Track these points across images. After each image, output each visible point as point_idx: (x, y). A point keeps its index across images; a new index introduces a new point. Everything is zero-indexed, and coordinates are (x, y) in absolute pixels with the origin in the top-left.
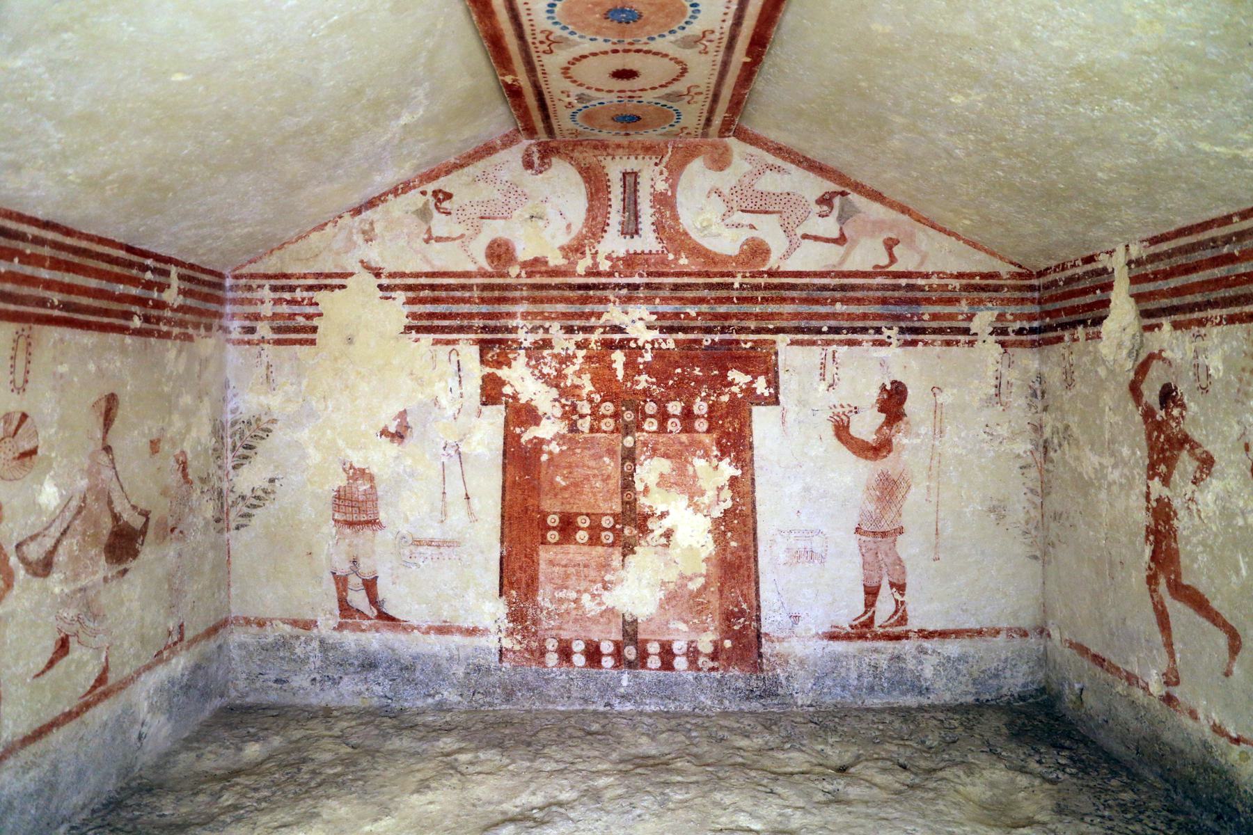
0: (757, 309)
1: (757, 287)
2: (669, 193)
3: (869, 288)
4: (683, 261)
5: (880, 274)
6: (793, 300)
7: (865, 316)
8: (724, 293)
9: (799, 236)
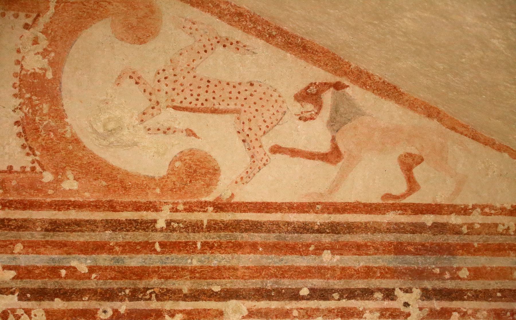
0: (194, 261)
1: (196, 227)
2: (49, 75)
3: (376, 229)
4: (70, 184)
5: (394, 208)
6: (254, 247)
7: (368, 272)
8: (139, 236)
9: (267, 148)
